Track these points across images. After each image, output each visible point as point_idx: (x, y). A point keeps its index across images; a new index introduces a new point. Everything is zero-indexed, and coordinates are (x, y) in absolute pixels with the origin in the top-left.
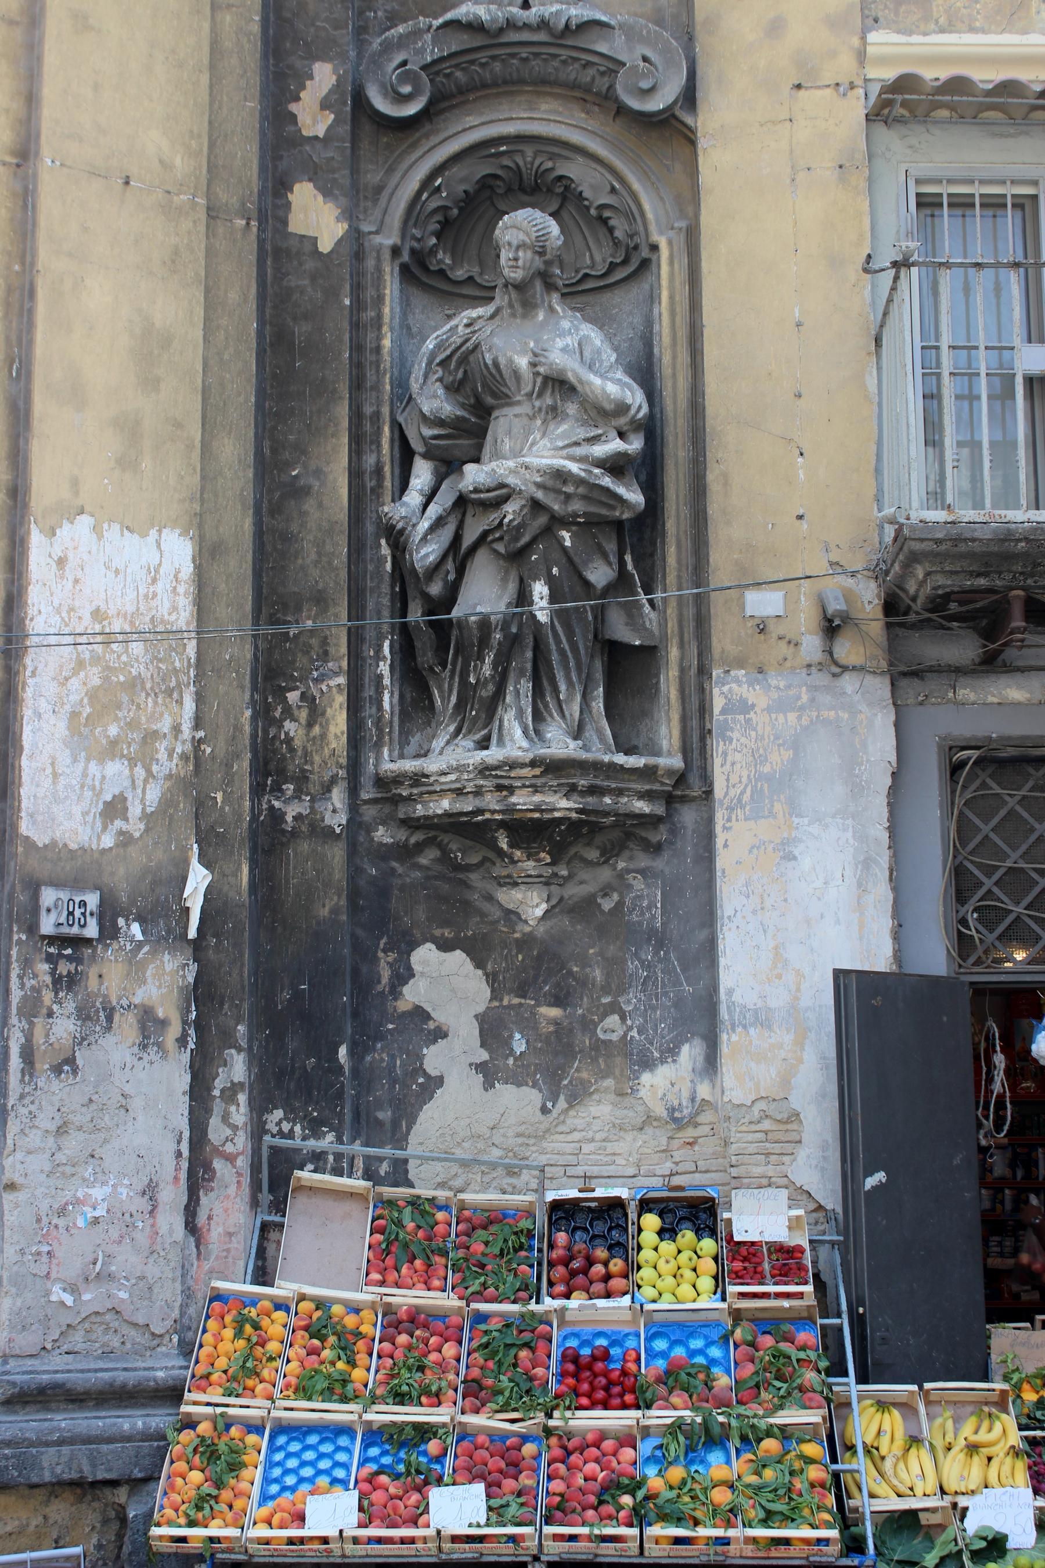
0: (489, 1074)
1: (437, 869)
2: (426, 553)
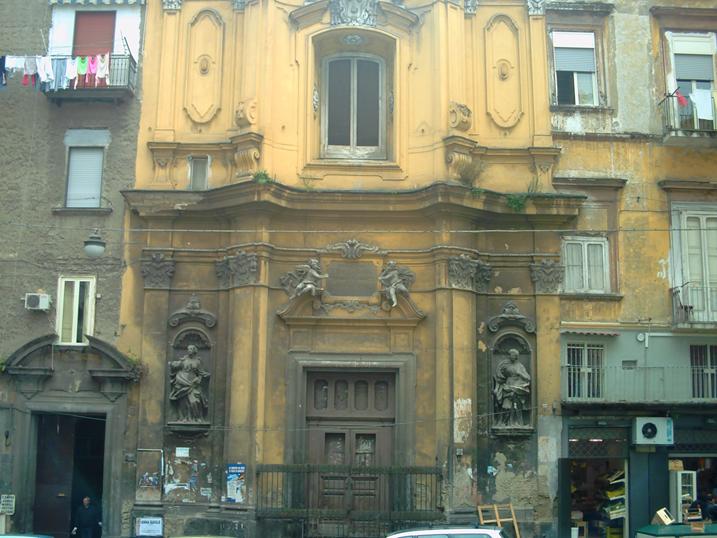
0: (506, 470)
1: (503, 440)
2: (499, 398)
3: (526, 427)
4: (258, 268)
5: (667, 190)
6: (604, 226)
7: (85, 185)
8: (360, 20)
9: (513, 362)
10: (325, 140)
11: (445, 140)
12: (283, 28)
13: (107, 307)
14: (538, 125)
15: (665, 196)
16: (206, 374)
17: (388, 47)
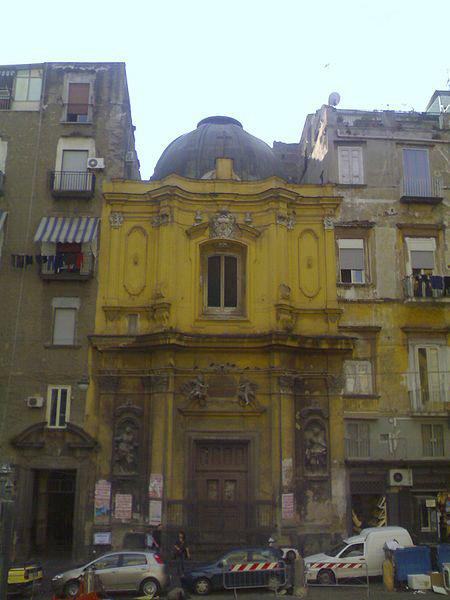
1: (309, 483)
3: (324, 475)
4: (168, 382)
5: (406, 332)
6: (368, 354)
7: (65, 331)
8: (227, 234)
9: (316, 435)
10: (206, 304)
11: (276, 306)
12: (183, 238)
13: (78, 405)
14: (329, 294)
15: (405, 336)
16: (136, 444)
17: (243, 249)
